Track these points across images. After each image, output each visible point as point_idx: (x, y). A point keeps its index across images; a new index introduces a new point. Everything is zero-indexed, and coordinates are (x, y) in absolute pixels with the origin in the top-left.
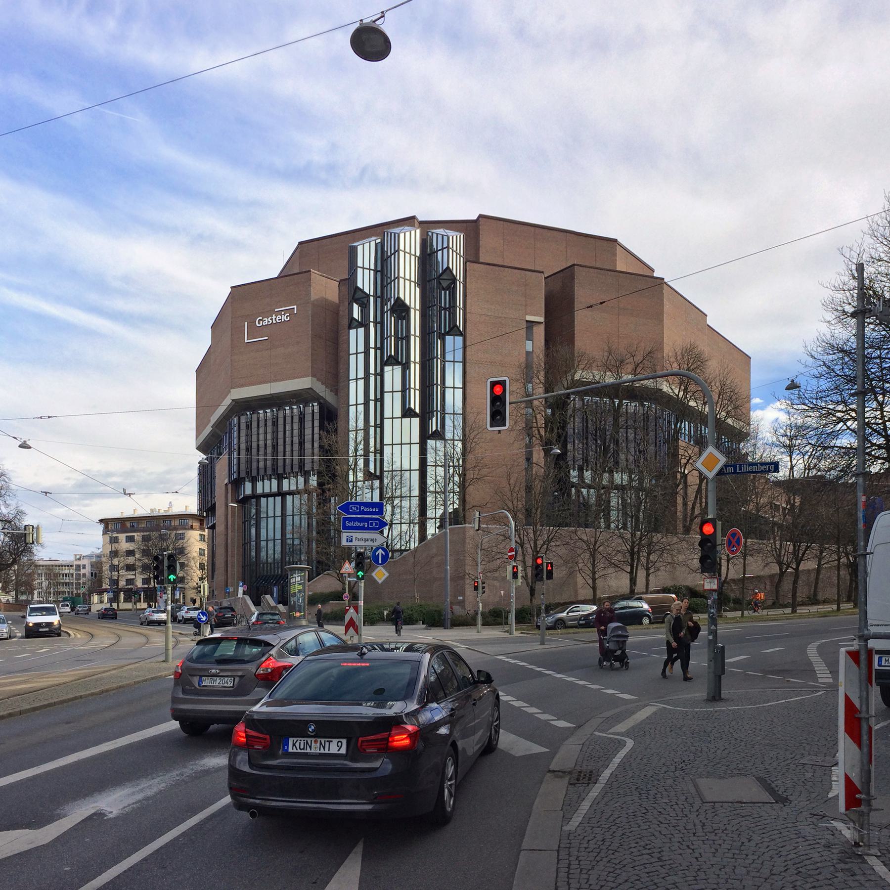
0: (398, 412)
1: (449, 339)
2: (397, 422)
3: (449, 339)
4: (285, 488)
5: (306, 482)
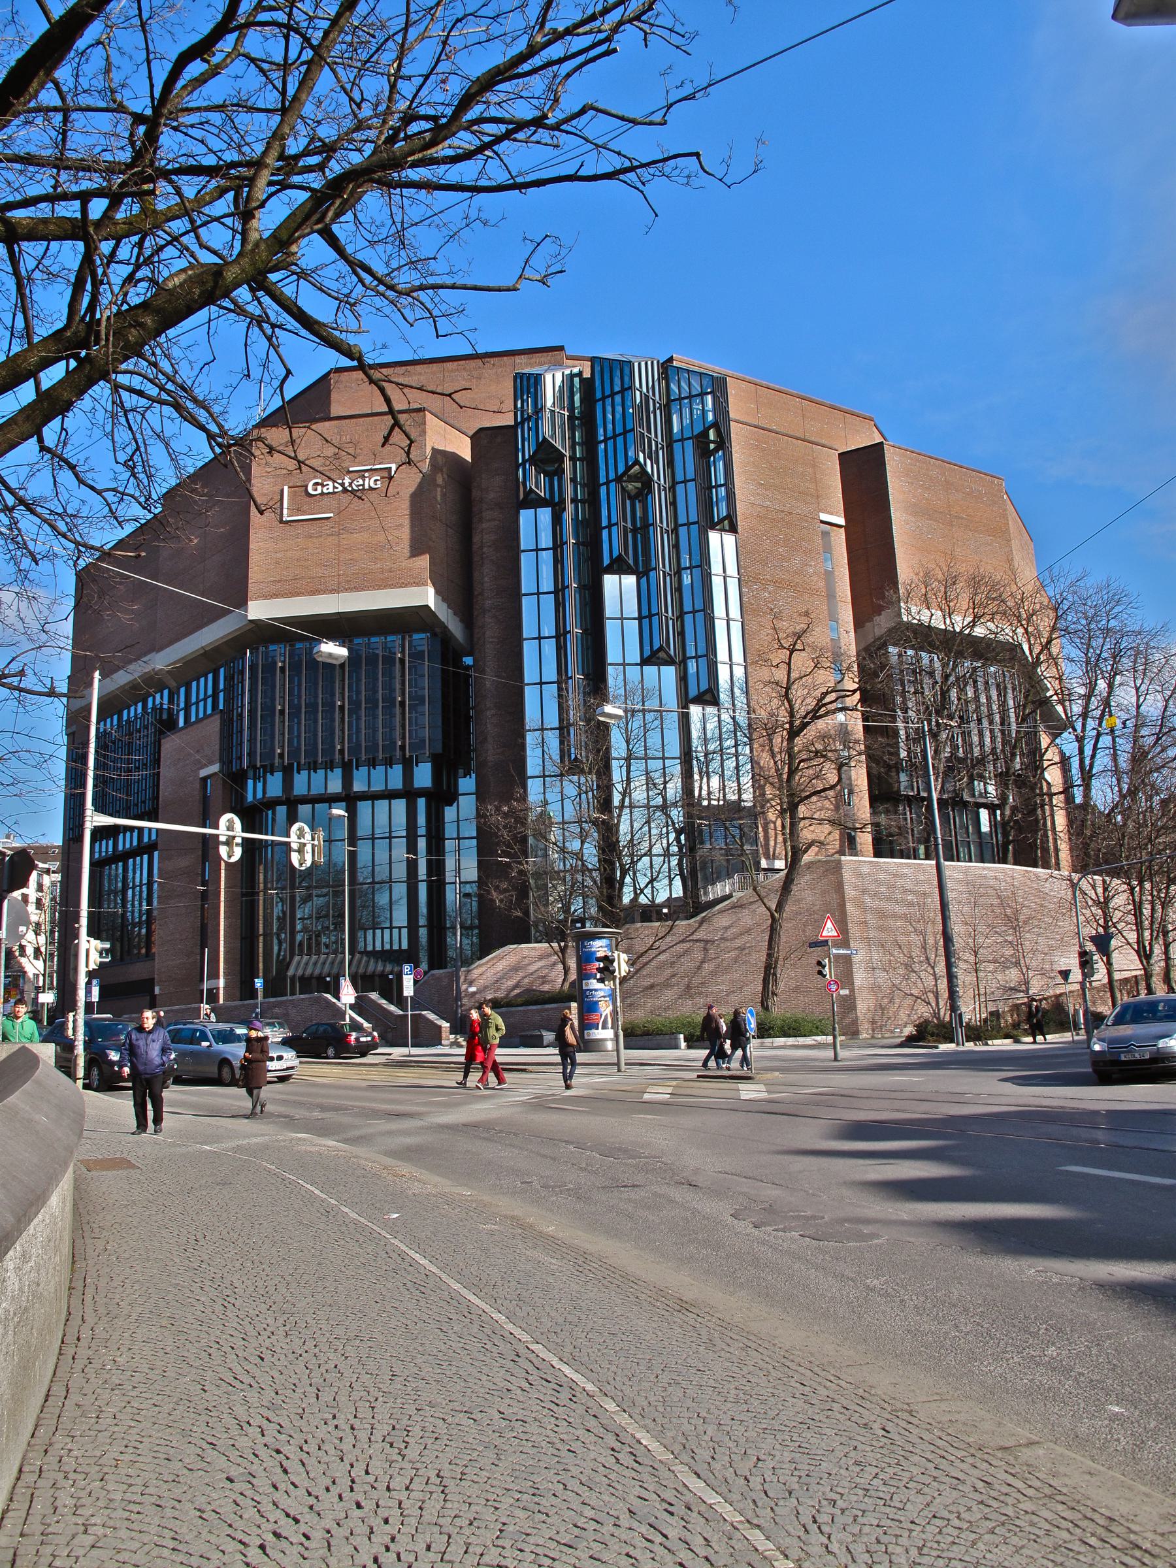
0: (634, 656)
1: (714, 537)
2: (633, 673)
3: (714, 537)
4: (358, 787)
5: (408, 776)
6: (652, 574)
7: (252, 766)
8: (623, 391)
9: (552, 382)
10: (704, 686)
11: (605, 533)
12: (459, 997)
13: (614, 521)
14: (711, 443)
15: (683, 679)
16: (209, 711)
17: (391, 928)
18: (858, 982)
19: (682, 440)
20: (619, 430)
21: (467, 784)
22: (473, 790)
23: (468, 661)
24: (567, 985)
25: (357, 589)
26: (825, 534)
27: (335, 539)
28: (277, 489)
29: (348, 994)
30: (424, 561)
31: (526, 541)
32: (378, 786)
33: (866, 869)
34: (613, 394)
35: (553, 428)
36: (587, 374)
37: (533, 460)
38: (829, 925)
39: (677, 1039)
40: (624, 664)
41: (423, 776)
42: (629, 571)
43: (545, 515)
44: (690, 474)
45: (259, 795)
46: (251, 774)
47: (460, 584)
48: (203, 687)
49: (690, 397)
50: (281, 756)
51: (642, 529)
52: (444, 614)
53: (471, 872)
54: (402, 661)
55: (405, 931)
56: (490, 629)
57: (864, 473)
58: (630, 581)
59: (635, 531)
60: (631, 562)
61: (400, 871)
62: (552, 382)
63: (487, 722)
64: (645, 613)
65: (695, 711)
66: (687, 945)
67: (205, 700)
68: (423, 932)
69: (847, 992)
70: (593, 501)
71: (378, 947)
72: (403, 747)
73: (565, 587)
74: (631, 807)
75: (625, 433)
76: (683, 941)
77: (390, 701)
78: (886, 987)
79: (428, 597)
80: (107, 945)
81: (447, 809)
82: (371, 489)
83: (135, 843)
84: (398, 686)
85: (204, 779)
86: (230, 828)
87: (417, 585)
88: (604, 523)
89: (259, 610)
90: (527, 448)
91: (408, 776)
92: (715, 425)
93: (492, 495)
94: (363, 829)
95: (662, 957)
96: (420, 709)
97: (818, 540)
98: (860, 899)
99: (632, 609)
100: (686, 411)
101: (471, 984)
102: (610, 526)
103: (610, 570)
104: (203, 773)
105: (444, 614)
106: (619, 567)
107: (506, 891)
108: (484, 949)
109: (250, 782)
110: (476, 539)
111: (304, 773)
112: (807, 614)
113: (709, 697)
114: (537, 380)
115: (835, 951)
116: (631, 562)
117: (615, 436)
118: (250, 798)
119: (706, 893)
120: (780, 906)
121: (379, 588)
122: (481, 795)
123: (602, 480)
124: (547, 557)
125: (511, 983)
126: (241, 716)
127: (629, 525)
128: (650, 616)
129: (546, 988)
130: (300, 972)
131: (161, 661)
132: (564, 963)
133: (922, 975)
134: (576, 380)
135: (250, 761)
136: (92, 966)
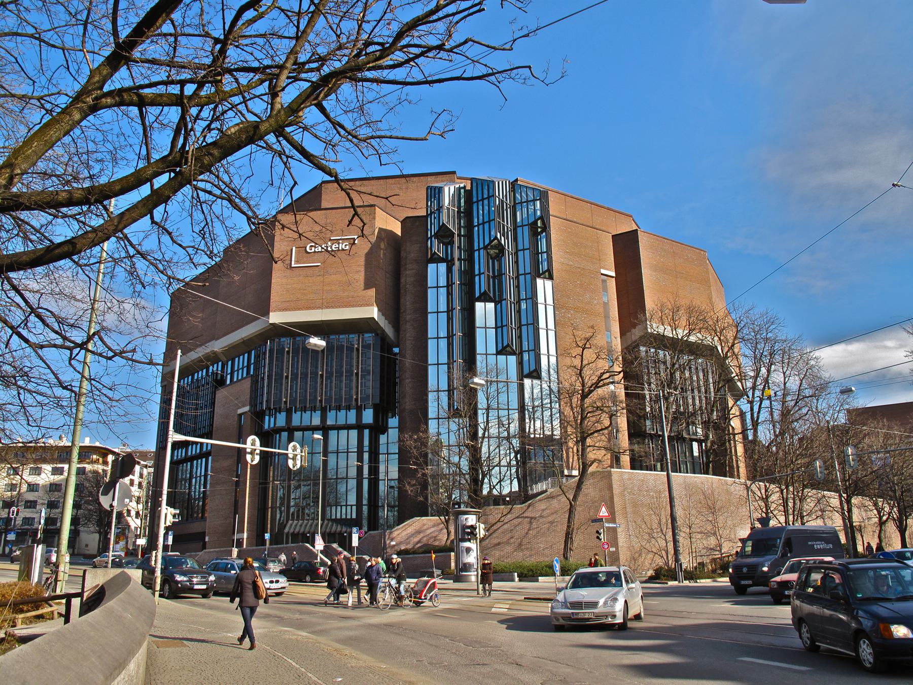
0: (492, 349)
1: (539, 282)
3: (539, 282)
4: (330, 422)
5: (359, 416)
6: (504, 302)
7: (269, 408)
8: (489, 197)
9: (449, 191)
10: (533, 368)
11: (477, 278)
12: (385, 548)
13: (482, 271)
14: (539, 228)
15: (520, 363)
16: (245, 375)
17: (346, 505)
18: (620, 544)
19: (522, 226)
20: (486, 219)
21: (393, 422)
22: (397, 425)
23: (396, 350)
24: (449, 542)
25: (333, 307)
26: (604, 281)
27: (320, 279)
28: (289, 248)
29: (319, 544)
30: (372, 292)
31: (431, 282)
32: (341, 421)
33: (626, 476)
34: (483, 199)
35: (448, 219)
36: (468, 188)
37: (436, 235)
38: (604, 509)
39: (513, 576)
40: (486, 354)
41: (368, 416)
42: (490, 300)
43: (443, 267)
44: (527, 246)
45: (272, 425)
46: (267, 412)
47: (393, 306)
48: (241, 361)
49: (527, 202)
50: (286, 402)
51: (498, 276)
52: (383, 323)
53: (394, 473)
54: (358, 350)
55: (354, 508)
56: (409, 333)
57: (626, 248)
58: (491, 306)
59: (494, 277)
60: (492, 295)
61: (353, 472)
62: (449, 191)
63: (406, 386)
64: (499, 324)
65: (527, 382)
66: (520, 520)
67: (243, 369)
68: (365, 509)
69: (614, 549)
70: (470, 260)
71: (338, 516)
72: (356, 400)
73: (453, 309)
74: (489, 437)
75: (489, 221)
76: (518, 517)
77: (350, 372)
78: (637, 546)
79: (374, 312)
80: (178, 512)
81: (381, 436)
82: (343, 250)
83: (198, 451)
84: (355, 364)
85: (240, 415)
86: (253, 444)
87: (368, 305)
88: (477, 272)
89: (276, 318)
90: (433, 229)
91: (359, 416)
92: (541, 218)
93: (412, 255)
94: (332, 446)
95: (505, 526)
96: (367, 377)
97: (600, 285)
98: (622, 494)
99: (491, 322)
100: (525, 210)
101: (392, 540)
102: (480, 274)
103: (479, 299)
104: (240, 411)
105: (383, 323)
106: (485, 298)
107: (414, 485)
108: (401, 520)
109: (267, 418)
110: (403, 280)
111: (299, 413)
112: (592, 327)
113: (535, 374)
114: (440, 190)
115: (607, 525)
116: (492, 295)
117: (484, 223)
118: (266, 427)
119: (532, 489)
120: (575, 497)
121: (346, 307)
122: (401, 428)
123: (476, 247)
124: (443, 291)
125: (416, 540)
126: (263, 379)
127: (491, 274)
128: (502, 327)
129: (437, 543)
130: (292, 531)
131: (218, 346)
132: (447, 529)
133: (659, 540)
134: (462, 191)
135: (267, 405)
136: (168, 524)
